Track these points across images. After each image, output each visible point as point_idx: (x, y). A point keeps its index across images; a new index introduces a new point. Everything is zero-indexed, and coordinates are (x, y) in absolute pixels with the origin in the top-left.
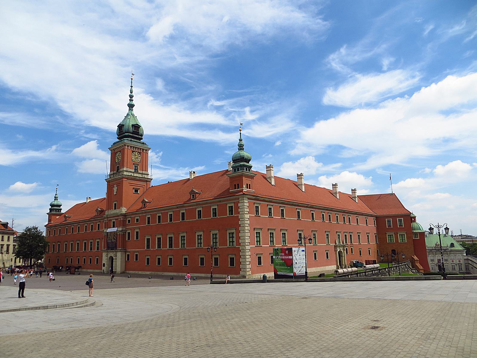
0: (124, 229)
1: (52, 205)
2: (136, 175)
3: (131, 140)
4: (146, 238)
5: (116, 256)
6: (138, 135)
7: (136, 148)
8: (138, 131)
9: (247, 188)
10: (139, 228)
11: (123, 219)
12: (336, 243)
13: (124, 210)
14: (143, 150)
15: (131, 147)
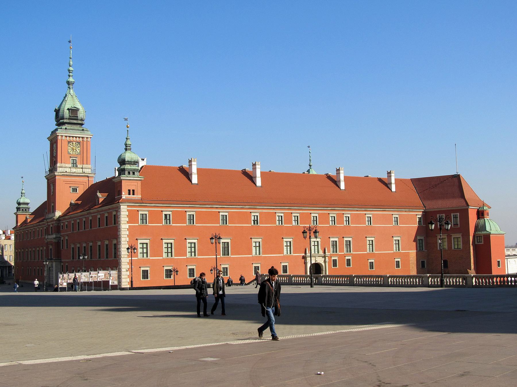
0: (59, 236)
1: (19, 204)
2: (74, 170)
3: (66, 128)
4: (72, 246)
5: (52, 267)
6: (77, 120)
7: (73, 137)
8: (77, 114)
9: (129, 194)
10: (67, 235)
11: (57, 225)
12: (305, 253)
13: (58, 214)
14: (83, 138)
15: (66, 136)
